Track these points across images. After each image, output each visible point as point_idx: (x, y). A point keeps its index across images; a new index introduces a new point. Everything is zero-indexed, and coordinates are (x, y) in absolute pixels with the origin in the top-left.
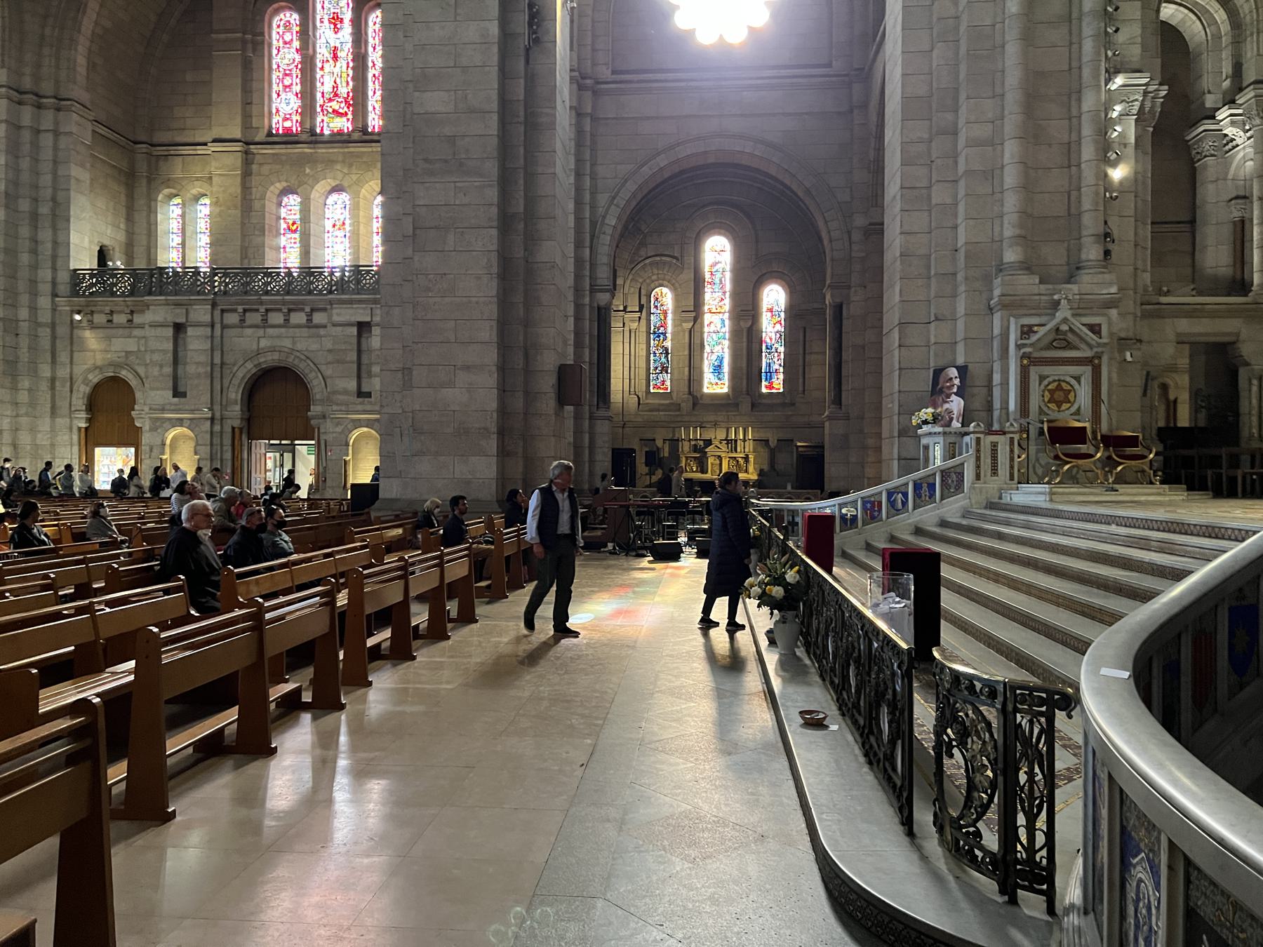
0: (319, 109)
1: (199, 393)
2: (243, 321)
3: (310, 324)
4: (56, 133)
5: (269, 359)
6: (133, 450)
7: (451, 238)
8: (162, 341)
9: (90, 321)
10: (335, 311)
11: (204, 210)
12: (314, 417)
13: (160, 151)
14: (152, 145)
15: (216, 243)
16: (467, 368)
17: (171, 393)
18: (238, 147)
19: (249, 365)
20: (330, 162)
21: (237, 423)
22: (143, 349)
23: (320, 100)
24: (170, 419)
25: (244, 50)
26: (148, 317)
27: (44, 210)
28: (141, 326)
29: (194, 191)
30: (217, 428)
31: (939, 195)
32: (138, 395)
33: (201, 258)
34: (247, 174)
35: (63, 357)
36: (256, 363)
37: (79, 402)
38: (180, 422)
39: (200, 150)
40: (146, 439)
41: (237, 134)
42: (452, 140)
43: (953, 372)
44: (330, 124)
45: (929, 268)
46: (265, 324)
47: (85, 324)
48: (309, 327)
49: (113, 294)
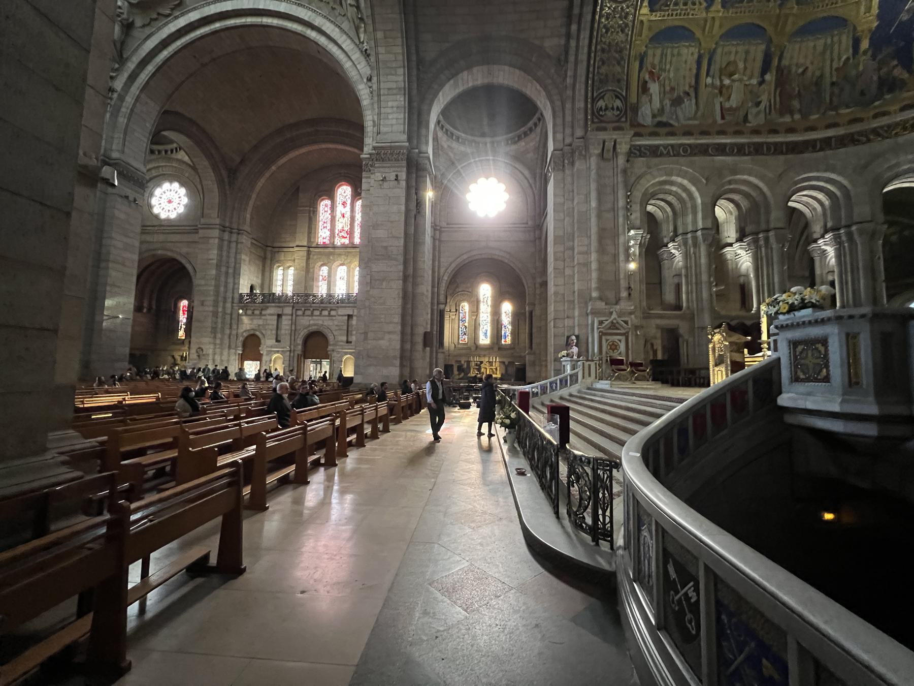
0: (336, 235)
1: (286, 340)
2: (304, 313)
3: (329, 315)
4: (237, 243)
5: (314, 328)
6: (259, 362)
7: (384, 283)
8: (273, 321)
9: (246, 313)
11: (291, 271)
12: (329, 351)
13: (277, 250)
14: (273, 247)
15: (296, 283)
16: (389, 333)
17: (274, 341)
18: (306, 249)
19: (305, 330)
20: (340, 255)
21: (300, 353)
23: (337, 232)
24: (273, 351)
25: (309, 214)
26: (269, 311)
27: (231, 271)
28: (265, 315)
29: (288, 265)
30: (292, 354)
31: (568, 272)
32: (262, 341)
33: (289, 291)
34: (308, 258)
35: (235, 327)
37: (240, 344)
38: (278, 352)
39: (291, 250)
40: (264, 358)
41: (305, 244)
42: (386, 248)
43: (574, 337)
44: (338, 242)
45: (564, 298)
46: (312, 315)
49: (255, 303)
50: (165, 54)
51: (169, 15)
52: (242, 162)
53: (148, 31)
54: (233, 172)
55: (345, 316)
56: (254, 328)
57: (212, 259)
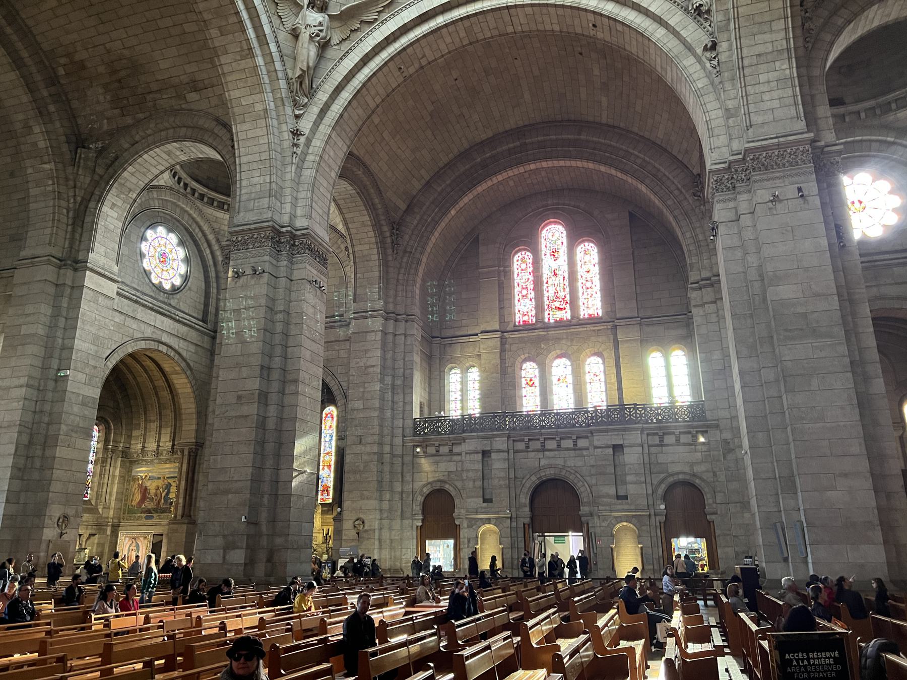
0: (546, 307)
1: (502, 498)
2: (527, 447)
3: (575, 447)
4: (405, 335)
5: (549, 473)
6: (451, 542)
8: (474, 464)
9: (425, 452)
10: (595, 438)
11: (474, 375)
12: (584, 515)
13: (448, 341)
14: (442, 338)
15: (485, 398)
17: (481, 500)
18: (498, 335)
19: (534, 478)
20: (558, 339)
21: (527, 520)
22: (459, 469)
23: (546, 302)
24: (481, 519)
25: (499, 276)
26: (464, 448)
27: (399, 382)
28: (460, 454)
29: (467, 365)
30: (514, 524)
32: (457, 501)
33: (475, 408)
34: (503, 351)
35: (408, 477)
36: (538, 476)
37: (418, 509)
38: (489, 521)
39: (472, 339)
40: (464, 533)
41: (497, 327)
42: (804, 315)
44: (552, 316)
46: (543, 449)
47: (422, 454)
48: (575, 450)
49: (439, 433)
50: (366, 72)
51: (376, 20)
52: (409, 209)
53: (345, 46)
54: (397, 227)
55: (608, 447)
56: (442, 478)
57: (373, 366)
